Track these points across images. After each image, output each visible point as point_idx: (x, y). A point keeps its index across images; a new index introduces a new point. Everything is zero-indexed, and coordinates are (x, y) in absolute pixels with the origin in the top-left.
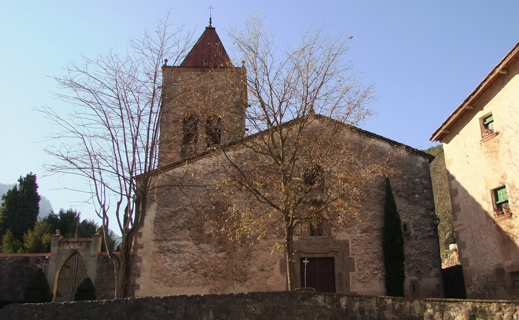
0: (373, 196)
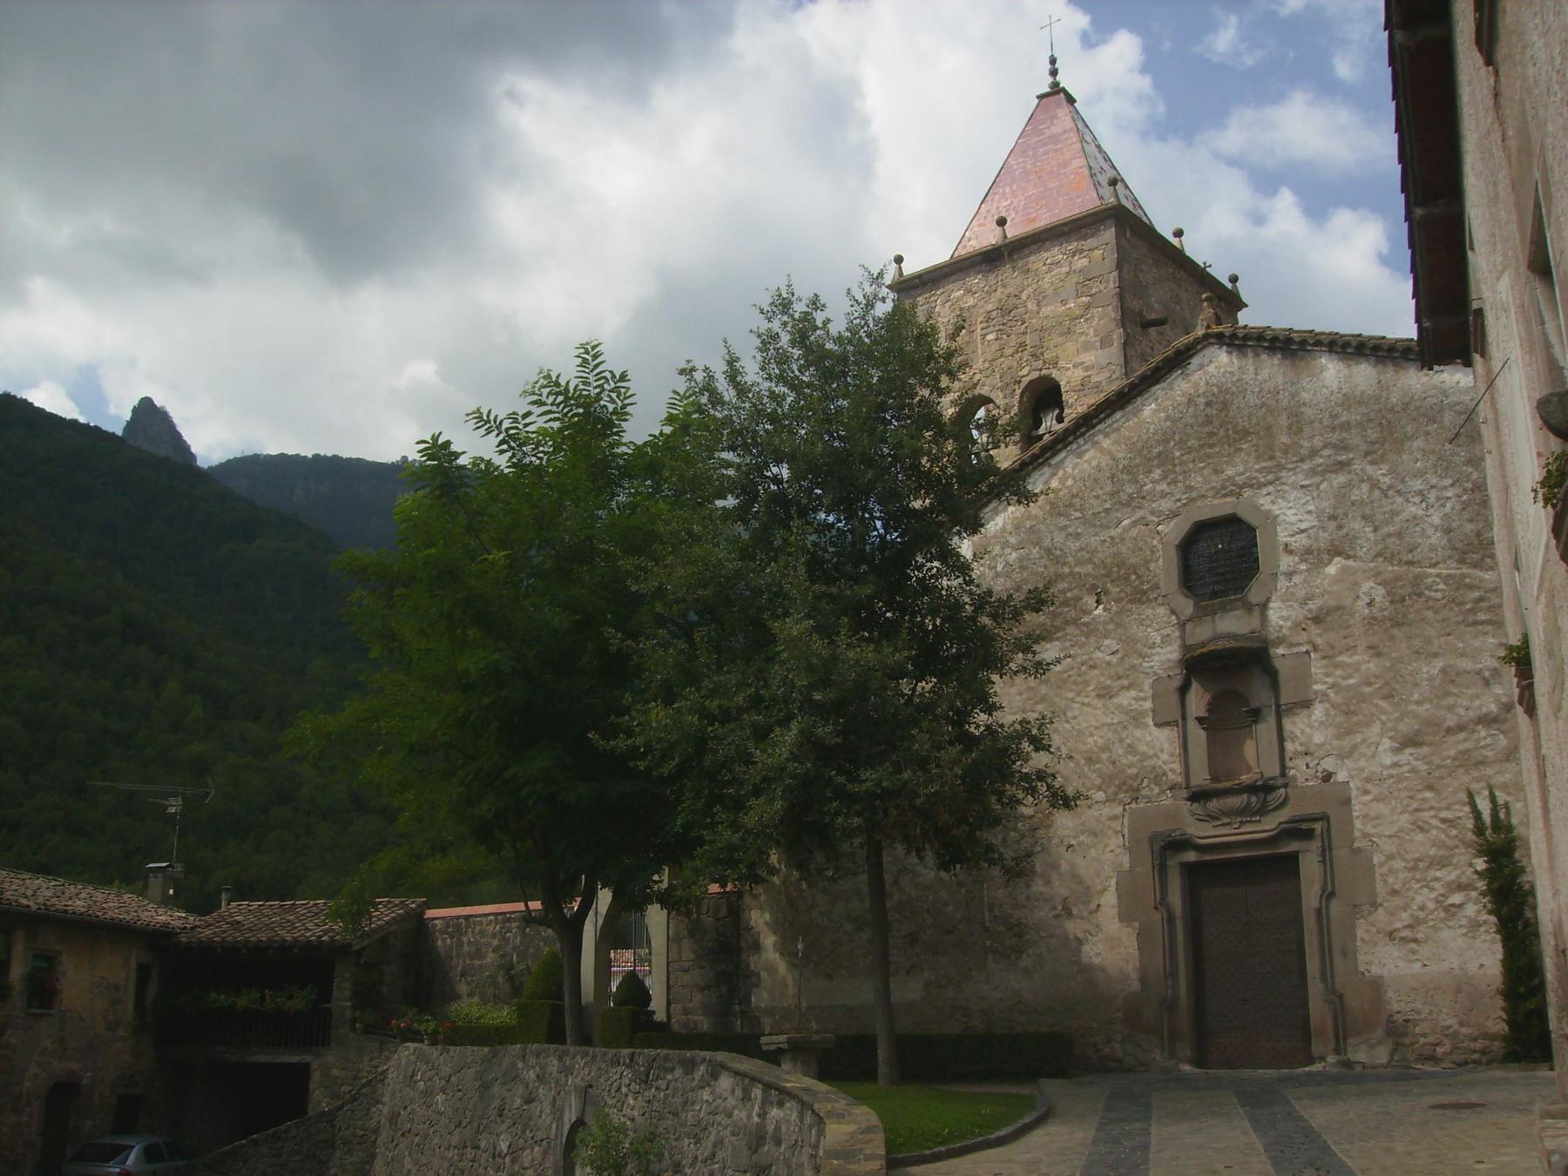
0: (1439, 595)
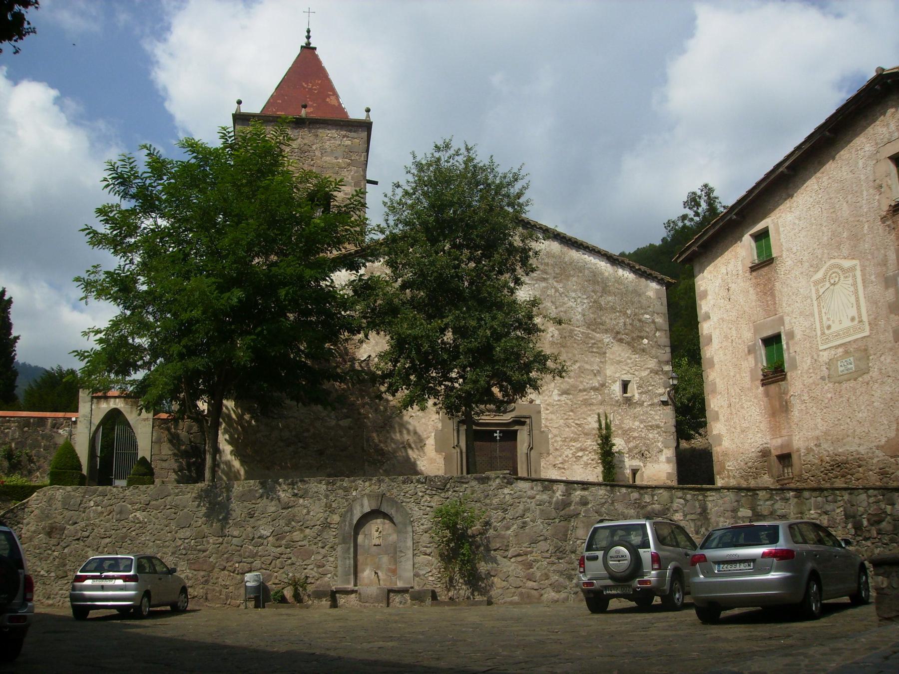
0: (579, 339)
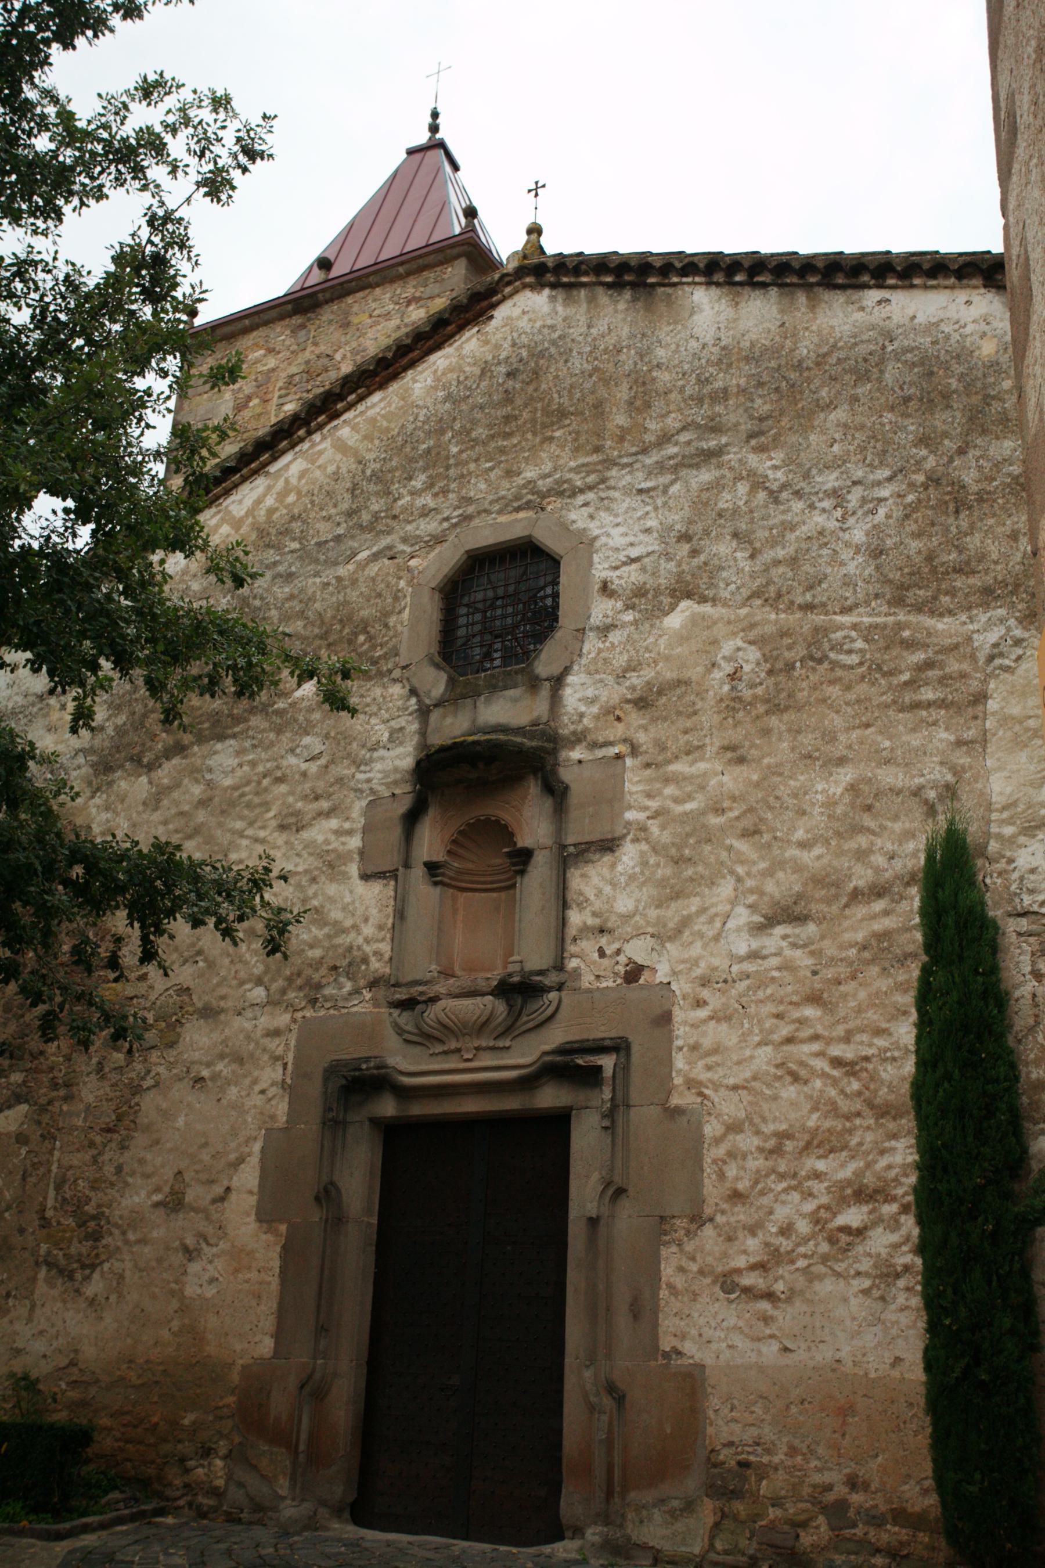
0: (854, 659)
